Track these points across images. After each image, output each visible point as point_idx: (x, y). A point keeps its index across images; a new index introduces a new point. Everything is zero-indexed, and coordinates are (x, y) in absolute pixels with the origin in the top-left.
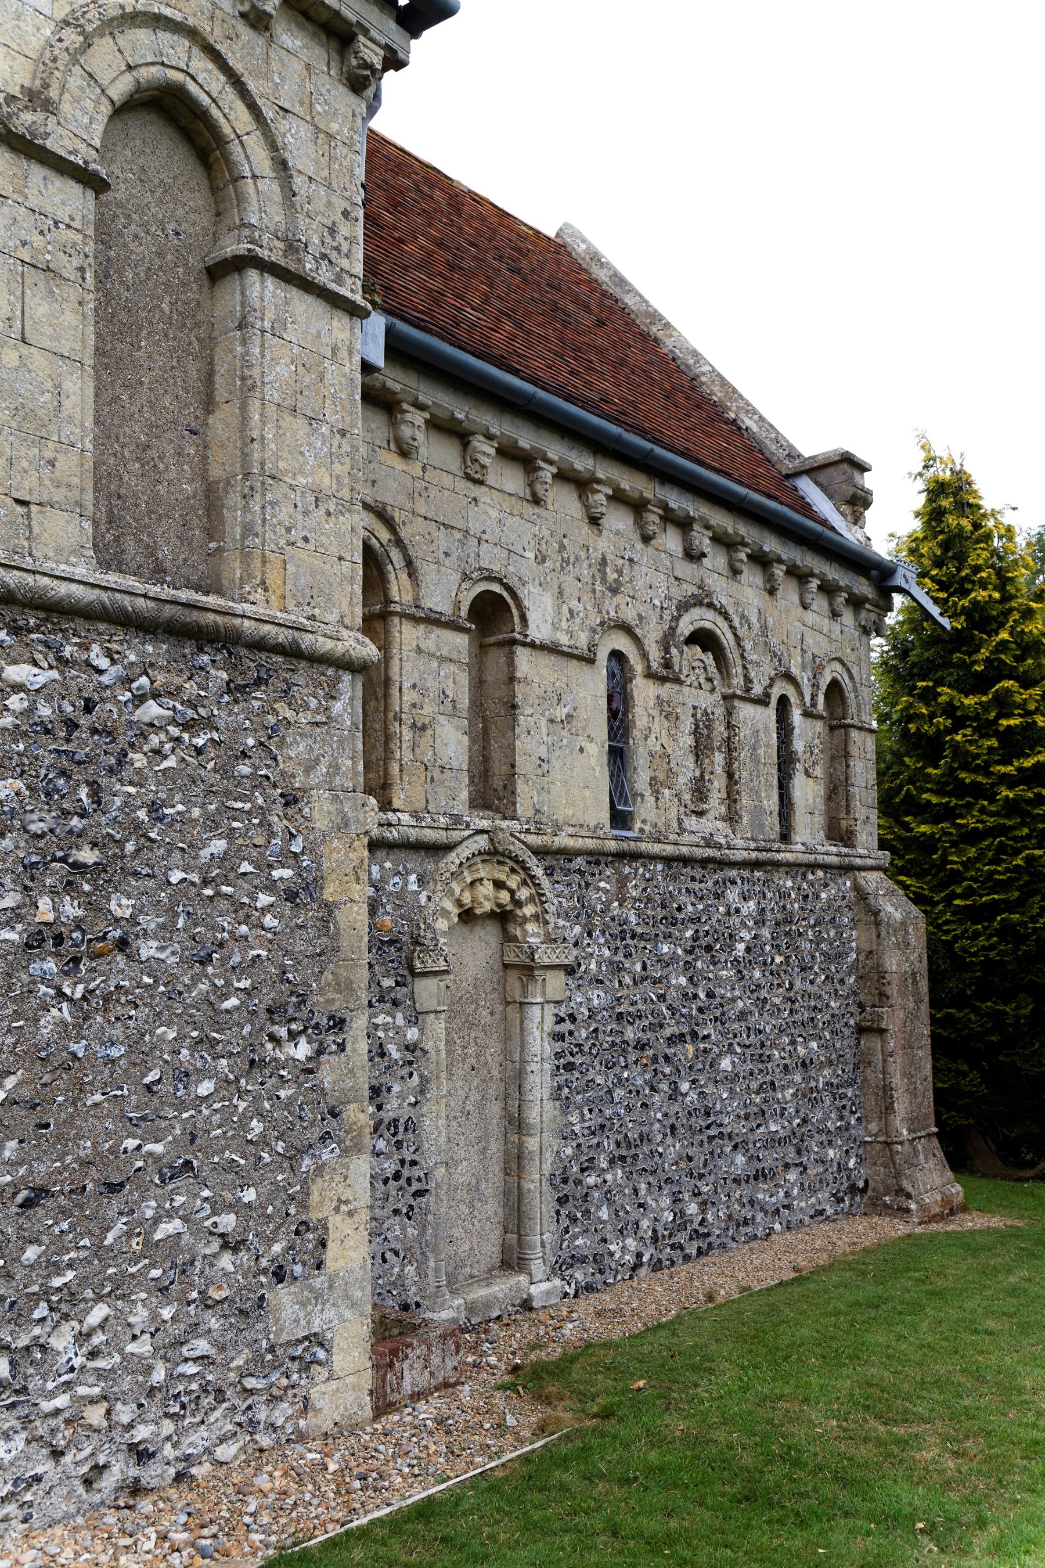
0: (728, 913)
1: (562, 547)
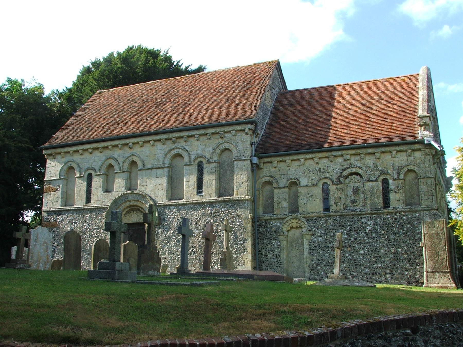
0: (362, 223)
1: (309, 170)
